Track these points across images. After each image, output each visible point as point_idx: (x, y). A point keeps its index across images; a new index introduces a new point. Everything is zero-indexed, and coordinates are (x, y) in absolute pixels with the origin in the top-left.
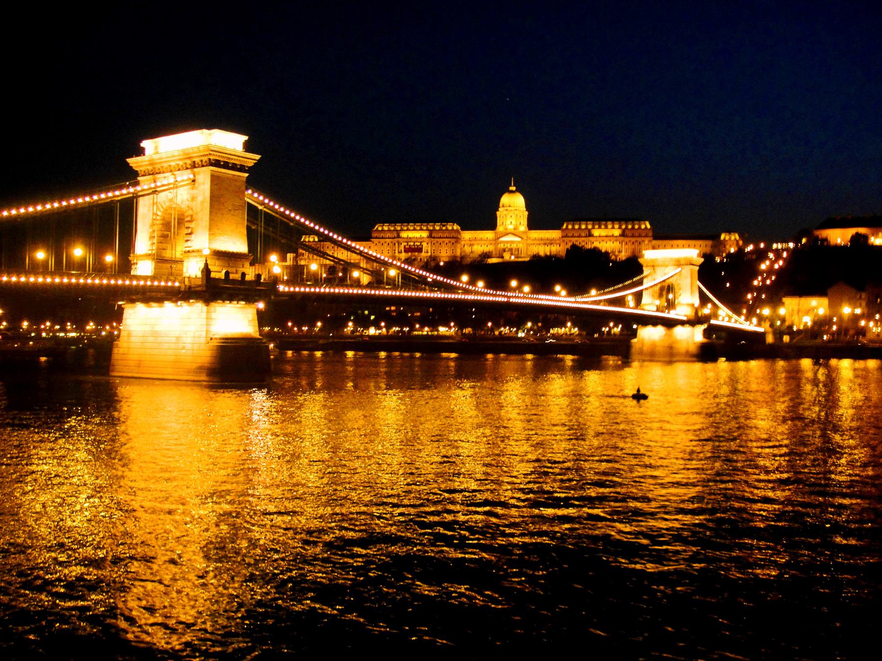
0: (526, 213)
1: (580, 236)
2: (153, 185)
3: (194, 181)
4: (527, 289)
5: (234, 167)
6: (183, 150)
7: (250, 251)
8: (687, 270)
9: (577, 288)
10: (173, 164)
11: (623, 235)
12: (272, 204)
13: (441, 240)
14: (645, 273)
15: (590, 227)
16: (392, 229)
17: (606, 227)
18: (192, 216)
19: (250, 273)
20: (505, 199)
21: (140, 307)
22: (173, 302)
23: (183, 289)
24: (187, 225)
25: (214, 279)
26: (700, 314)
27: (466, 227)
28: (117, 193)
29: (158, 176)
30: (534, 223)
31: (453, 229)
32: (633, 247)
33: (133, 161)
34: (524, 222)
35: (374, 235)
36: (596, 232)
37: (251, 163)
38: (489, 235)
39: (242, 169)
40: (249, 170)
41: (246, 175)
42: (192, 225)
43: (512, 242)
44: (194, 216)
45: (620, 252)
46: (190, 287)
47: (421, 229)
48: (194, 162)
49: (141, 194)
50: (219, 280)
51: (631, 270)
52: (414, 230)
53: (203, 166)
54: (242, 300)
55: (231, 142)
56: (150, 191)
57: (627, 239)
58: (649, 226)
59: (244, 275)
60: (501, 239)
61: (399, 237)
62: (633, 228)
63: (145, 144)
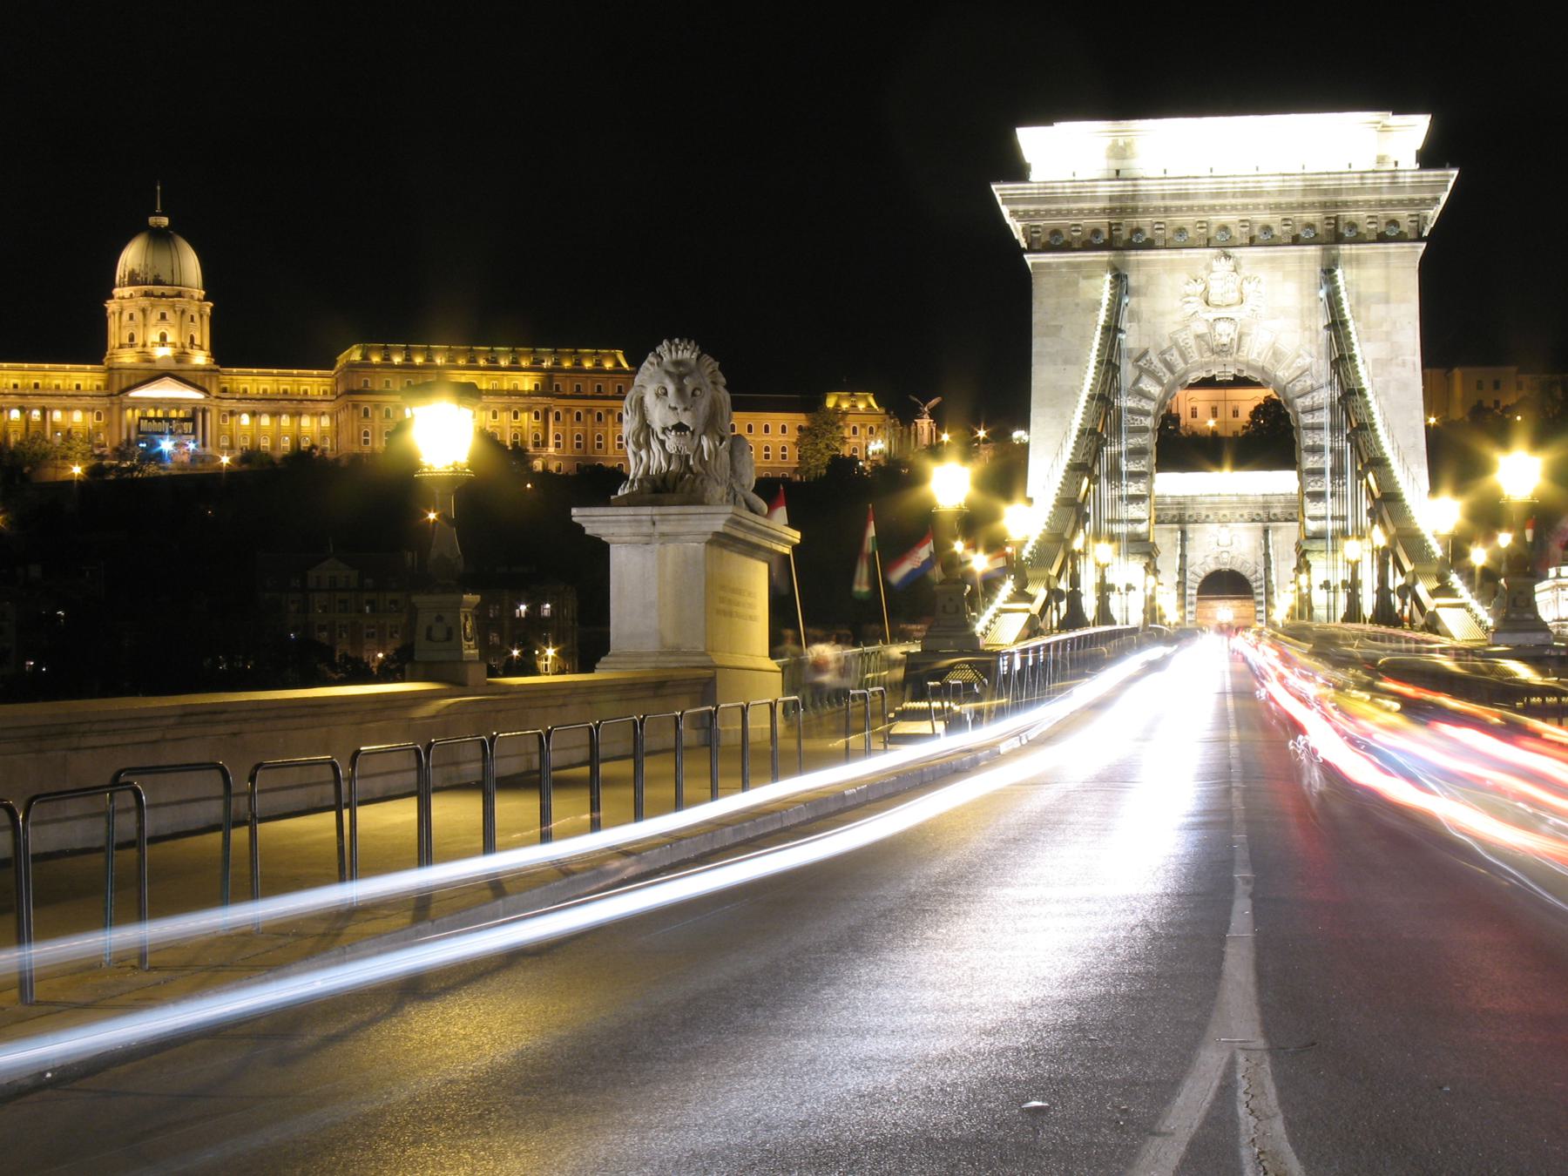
17: (493, 366)
20: (131, 257)
29: (1135, 256)
30: (233, 346)
32: (579, 428)
34: (202, 333)
38: (84, 377)
45: (541, 444)
48: (1336, 219)
53: (1382, 238)
57: (558, 405)
58: (625, 365)
60: (135, 394)
62: (578, 369)
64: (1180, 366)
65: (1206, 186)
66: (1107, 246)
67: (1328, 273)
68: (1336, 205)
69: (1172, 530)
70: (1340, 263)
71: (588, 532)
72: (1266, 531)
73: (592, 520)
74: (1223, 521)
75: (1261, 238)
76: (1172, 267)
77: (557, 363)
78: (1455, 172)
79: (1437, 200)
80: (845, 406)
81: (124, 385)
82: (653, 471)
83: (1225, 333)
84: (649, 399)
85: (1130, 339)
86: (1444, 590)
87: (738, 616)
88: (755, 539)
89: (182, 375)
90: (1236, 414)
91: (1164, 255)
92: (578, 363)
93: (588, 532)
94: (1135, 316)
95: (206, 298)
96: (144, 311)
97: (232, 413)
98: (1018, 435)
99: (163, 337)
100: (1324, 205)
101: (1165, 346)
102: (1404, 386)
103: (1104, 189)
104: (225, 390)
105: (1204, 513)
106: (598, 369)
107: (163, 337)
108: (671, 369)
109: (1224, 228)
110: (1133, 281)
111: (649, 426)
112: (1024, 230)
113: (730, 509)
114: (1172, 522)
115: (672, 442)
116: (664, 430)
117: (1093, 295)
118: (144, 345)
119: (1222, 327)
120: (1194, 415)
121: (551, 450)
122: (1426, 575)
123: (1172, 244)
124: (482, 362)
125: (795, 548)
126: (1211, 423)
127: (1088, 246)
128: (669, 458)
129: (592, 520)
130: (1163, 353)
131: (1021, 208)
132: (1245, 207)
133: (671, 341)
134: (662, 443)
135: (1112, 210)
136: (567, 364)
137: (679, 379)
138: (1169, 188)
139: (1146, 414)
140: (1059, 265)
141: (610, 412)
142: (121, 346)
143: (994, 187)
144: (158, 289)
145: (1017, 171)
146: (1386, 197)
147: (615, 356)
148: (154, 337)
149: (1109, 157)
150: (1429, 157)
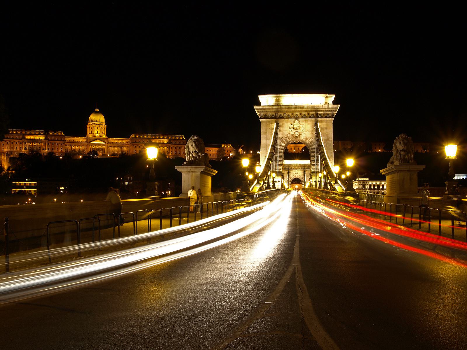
13: (53, 142)
20: (92, 117)
27: (67, 134)
29: (280, 120)
30: (110, 133)
31: (61, 135)
34: (105, 131)
38: (82, 139)
43: (99, 145)
47: (40, 134)
48: (318, 113)
52: (35, 134)
53: (326, 117)
57: (171, 146)
58: (184, 138)
60: (92, 143)
62: (175, 139)
64: (288, 140)
65: (294, 107)
66: (275, 118)
67: (316, 124)
68: (318, 111)
69: (287, 171)
70: (318, 121)
71: (178, 171)
72: (304, 171)
73: (179, 168)
74: (296, 169)
75: (304, 117)
76: (287, 122)
77: (171, 138)
78: (340, 105)
79: (336, 110)
80: (226, 146)
81: (90, 141)
82: (190, 160)
83: (297, 134)
84: (190, 146)
85: (279, 135)
86: (336, 183)
87: (206, 187)
88: (209, 172)
89: (100, 139)
90: (299, 149)
91: (286, 120)
93: (178, 171)
94: (280, 131)
95: (105, 125)
96: (94, 127)
97: (110, 146)
98: (258, 152)
99: (97, 132)
100: (315, 111)
101: (286, 137)
102: (330, 145)
103: (275, 107)
104: (109, 142)
105: (293, 167)
106: (179, 139)
107: (97, 132)
108: (194, 141)
109: (297, 115)
110: (280, 124)
111: (190, 151)
112: (260, 114)
113: (205, 167)
114: (287, 169)
115: (194, 154)
116: (192, 152)
117: (272, 127)
118: (94, 134)
119: (296, 133)
120: (291, 149)
121: (170, 154)
122: (333, 180)
123: (287, 118)
125: (216, 174)
126: (294, 151)
128: (193, 157)
129: (179, 168)
130: (285, 138)
131: (259, 110)
132: (301, 111)
133: (194, 136)
134: (192, 154)
135: (276, 111)
137: (195, 142)
138: (287, 107)
139: (282, 149)
140: (266, 121)
142: (89, 134)
143: (254, 106)
145: (259, 103)
146: (326, 110)
147: (182, 136)
148: (96, 133)
149: (275, 101)
150: (334, 102)
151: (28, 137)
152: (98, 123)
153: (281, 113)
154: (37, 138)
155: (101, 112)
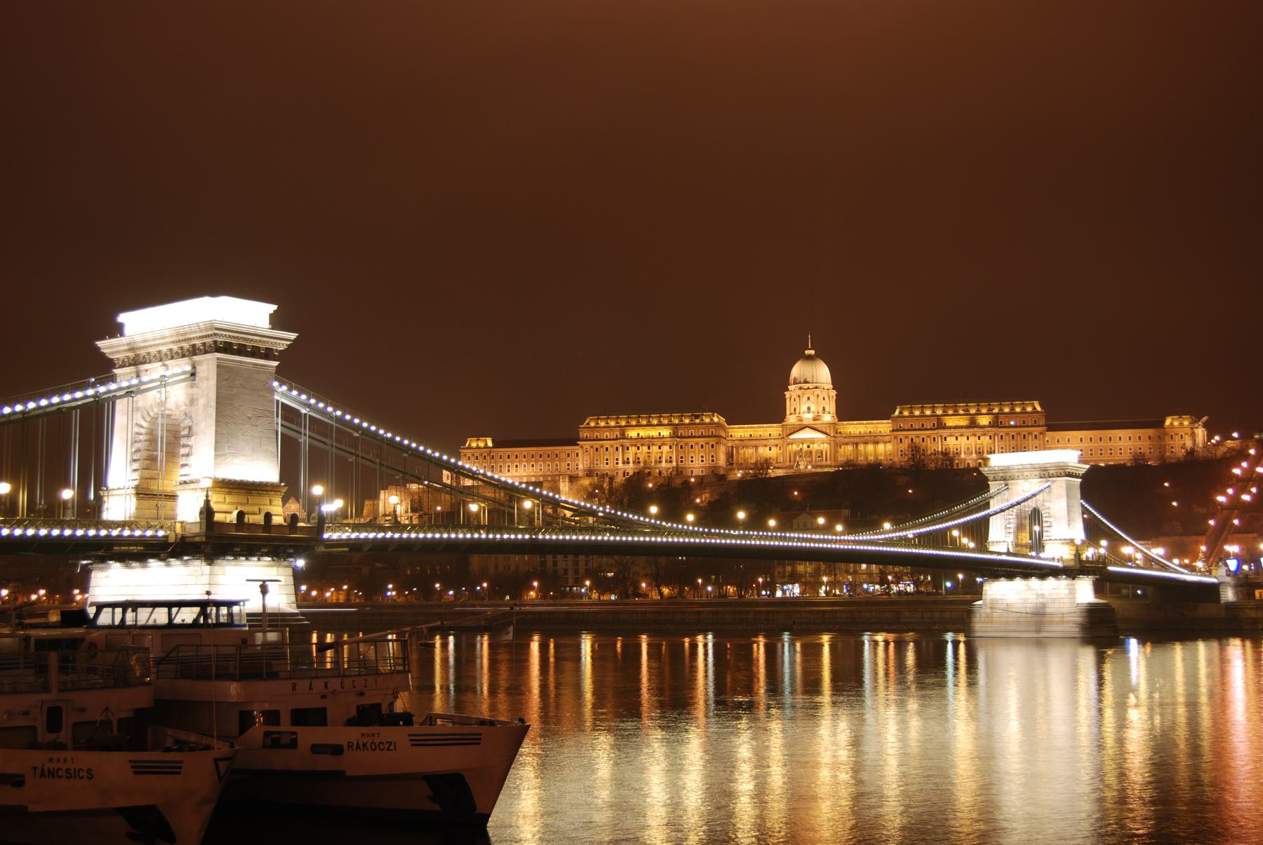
0: (834, 393)
1: (923, 429)
2: (135, 381)
3: (193, 374)
4: (772, 523)
5: (255, 352)
6: (176, 329)
7: (281, 480)
8: (1060, 484)
9: (862, 520)
10: (164, 349)
11: (995, 424)
12: (321, 405)
13: (692, 441)
14: (993, 490)
15: (939, 412)
16: (613, 423)
18: (190, 428)
19: (279, 513)
20: (797, 370)
21: (115, 568)
22: (161, 560)
23: (172, 539)
24: (183, 441)
25: (222, 524)
26: (1084, 557)
28: (79, 395)
30: (846, 411)
31: (712, 423)
33: (106, 345)
34: (831, 406)
35: (584, 434)
36: (950, 421)
37: (282, 346)
38: (772, 430)
39: (268, 354)
40: (281, 356)
41: (276, 364)
42: (191, 441)
43: (812, 441)
44: (194, 428)
46: (183, 538)
47: (660, 424)
48: (194, 346)
49: (118, 394)
50: (230, 524)
51: (963, 486)
52: (649, 425)
53: (206, 352)
54: (267, 555)
55: (252, 315)
56: (123, 392)
58: (1039, 409)
59: (268, 516)
61: (623, 437)
62: (1012, 412)
63: (123, 318)
92: (1012, 409)
106: (1024, 412)
124: (961, 412)
127: (130, 365)
132: (164, 344)
136: (1007, 410)
141: (1030, 433)
144: (806, 386)
148: (804, 408)
151: (633, 433)
152: (811, 386)
153: (142, 352)
154: (653, 433)
155: (822, 355)
